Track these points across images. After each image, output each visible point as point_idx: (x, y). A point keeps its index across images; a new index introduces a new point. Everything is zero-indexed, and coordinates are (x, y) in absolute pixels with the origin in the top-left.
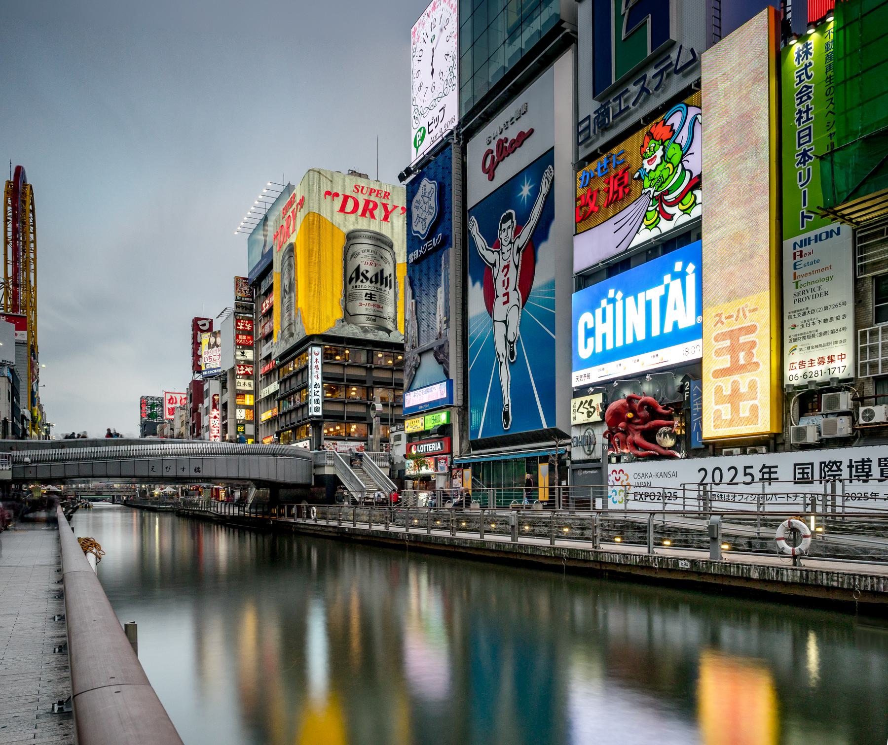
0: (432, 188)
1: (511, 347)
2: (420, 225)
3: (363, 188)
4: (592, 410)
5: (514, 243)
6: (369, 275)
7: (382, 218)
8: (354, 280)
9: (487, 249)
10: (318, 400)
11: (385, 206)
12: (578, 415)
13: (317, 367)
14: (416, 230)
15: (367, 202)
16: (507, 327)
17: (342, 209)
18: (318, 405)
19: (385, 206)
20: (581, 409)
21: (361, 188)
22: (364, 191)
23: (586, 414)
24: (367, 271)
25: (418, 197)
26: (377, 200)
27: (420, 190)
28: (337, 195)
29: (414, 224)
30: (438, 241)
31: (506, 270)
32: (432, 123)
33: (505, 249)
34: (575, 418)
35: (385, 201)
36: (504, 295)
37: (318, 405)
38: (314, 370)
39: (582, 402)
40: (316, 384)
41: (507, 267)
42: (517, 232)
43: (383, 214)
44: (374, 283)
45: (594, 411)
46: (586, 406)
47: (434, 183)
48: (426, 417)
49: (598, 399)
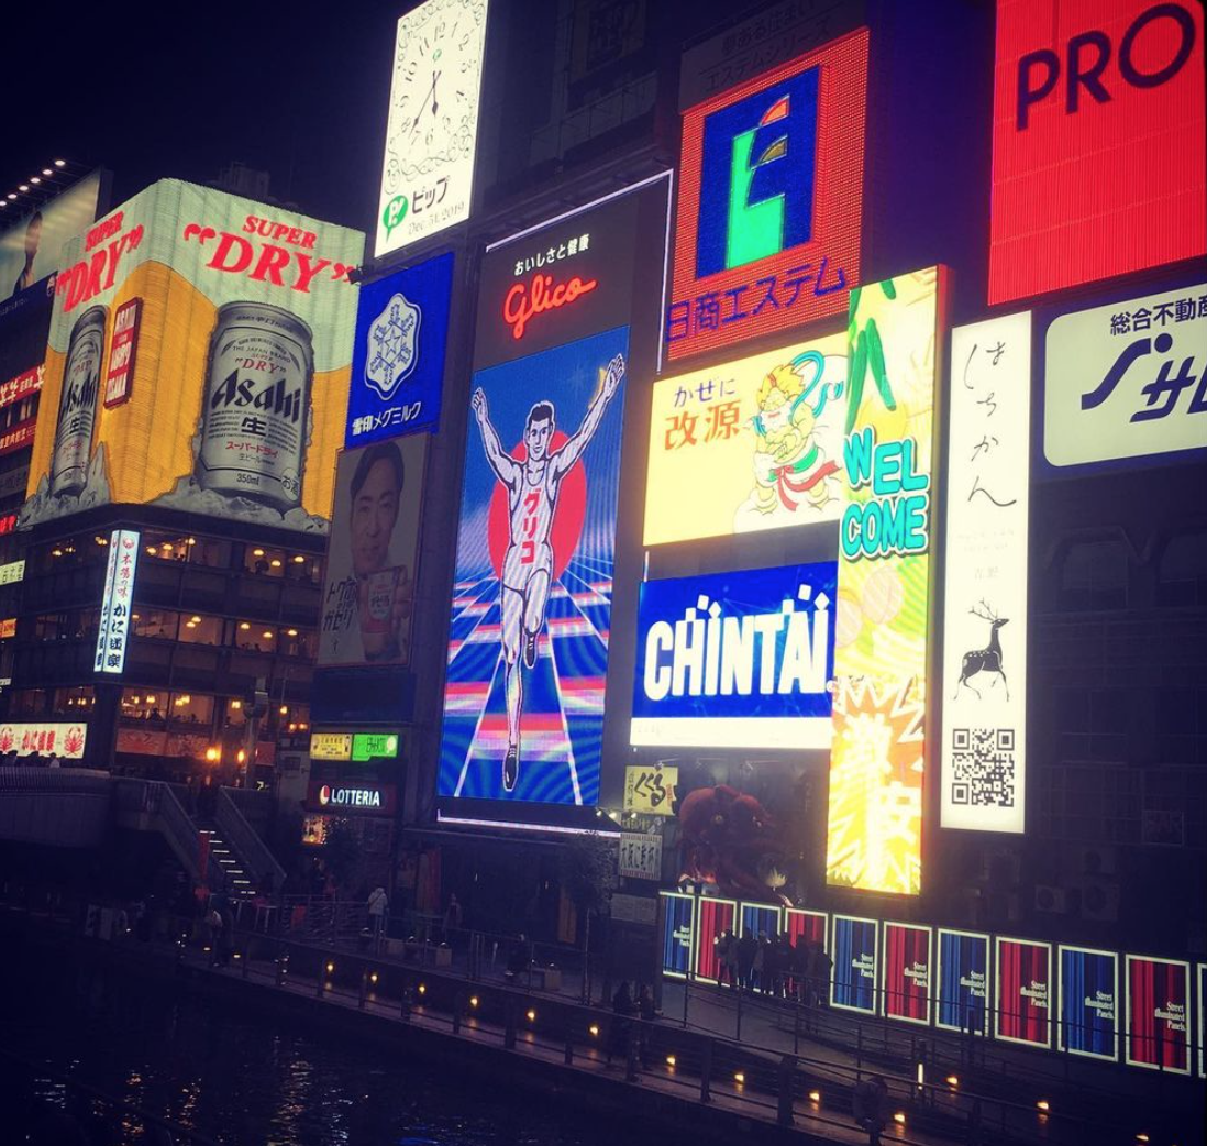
0: (411, 316)
1: (529, 642)
2: (380, 371)
3: (264, 222)
4: (660, 793)
5: (550, 460)
6: (254, 391)
7: (295, 283)
8: (224, 400)
9: (501, 455)
10: (118, 641)
11: (303, 260)
12: (637, 797)
13: (126, 570)
14: (371, 377)
15: (269, 251)
17: (218, 262)
18: (117, 652)
19: (303, 260)
20: (642, 788)
21: (259, 222)
22: (266, 229)
23: (649, 799)
24: (251, 383)
25: (383, 320)
26: (290, 248)
27: (388, 310)
28: (210, 233)
29: (369, 367)
30: (413, 413)
31: (532, 503)
32: (422, 196)
33: (534, 466)
34: (630, 801)
35: (304, 251)
36: (526, 545)
37: (117, 652)
38: (119, 578)
39: (644, 776)
40: (119, 608)
41: (534, 497)
42: (556, 447)
43: (298, 274)
44: (262, 408)
45: (664, 796)
46: (651, 783)
47: (415, 308)
48: (357, 736)
49: (670, 778)
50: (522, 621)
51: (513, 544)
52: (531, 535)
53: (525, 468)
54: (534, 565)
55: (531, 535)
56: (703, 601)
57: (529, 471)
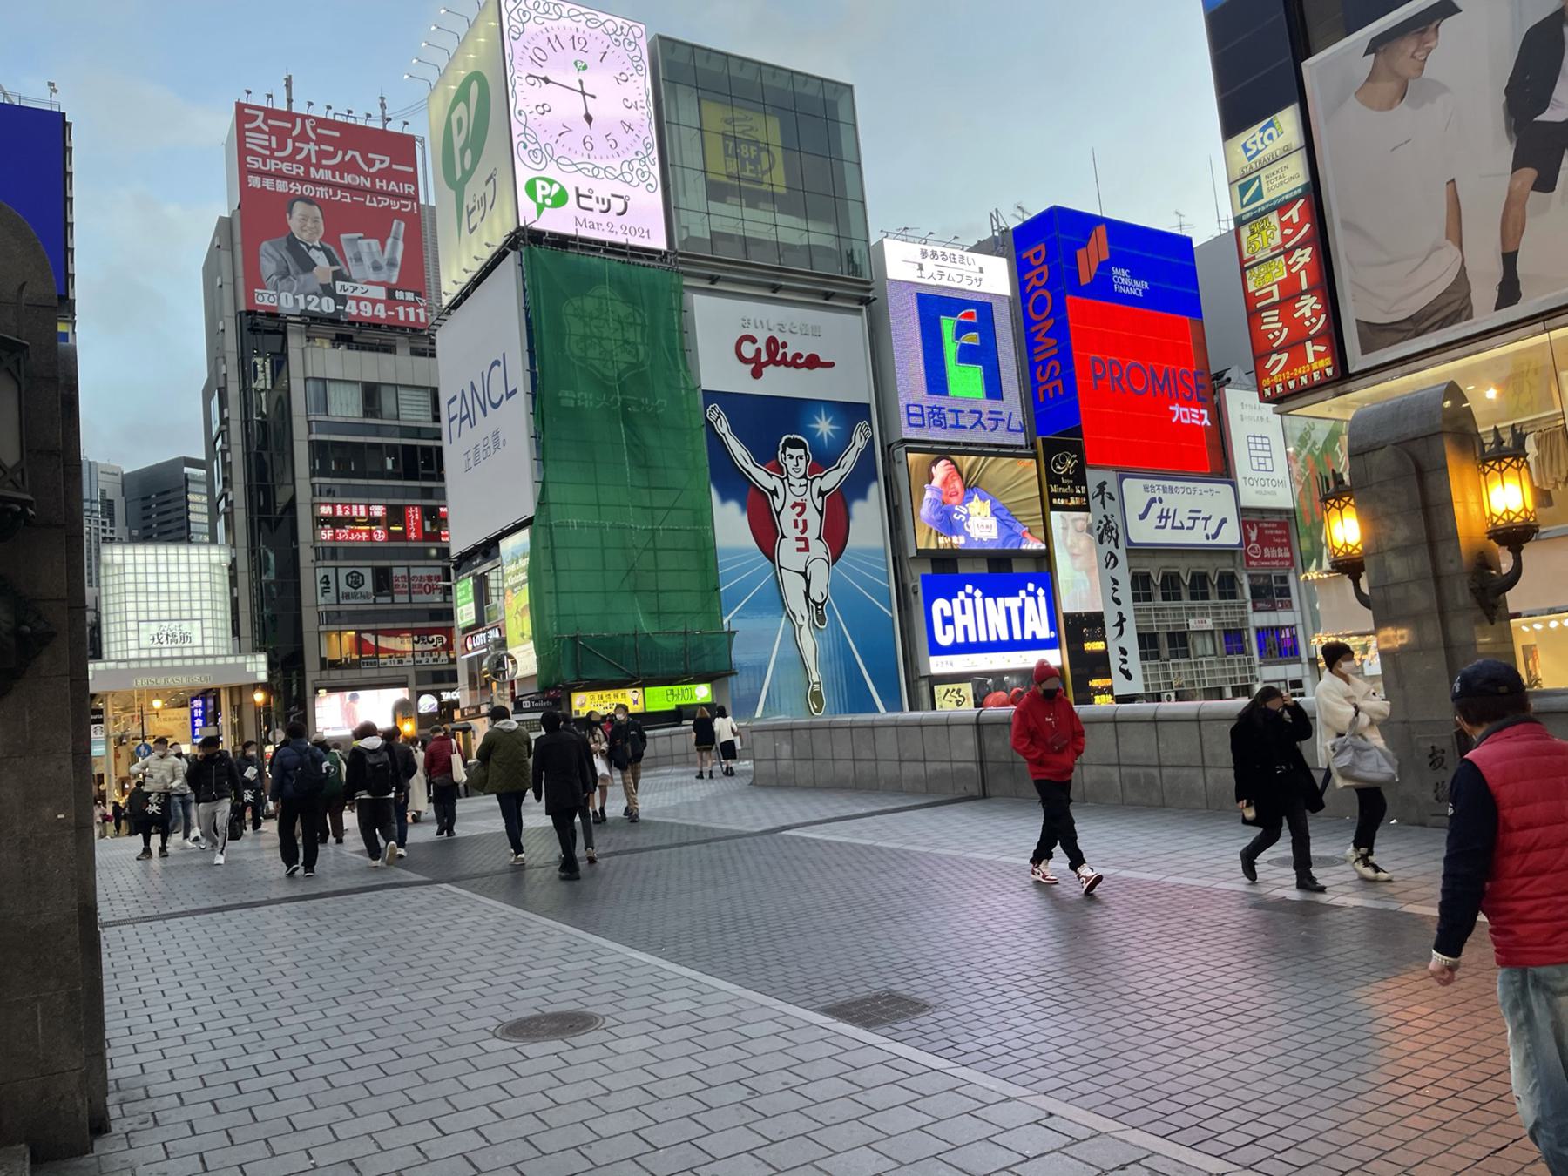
4: (961, 699)
12: (945, 703)
16: (808, 582)
20: (948, 697)
23: (954, 704)
34: (941, 707)
39: (948, 691)
50: (807, 594)
51: (784, 537)
52: (803, 532)
53: (786, 481)
54: (813, 553)
55: (803, 532)
56: (969, 588)
57: (790, 485)
